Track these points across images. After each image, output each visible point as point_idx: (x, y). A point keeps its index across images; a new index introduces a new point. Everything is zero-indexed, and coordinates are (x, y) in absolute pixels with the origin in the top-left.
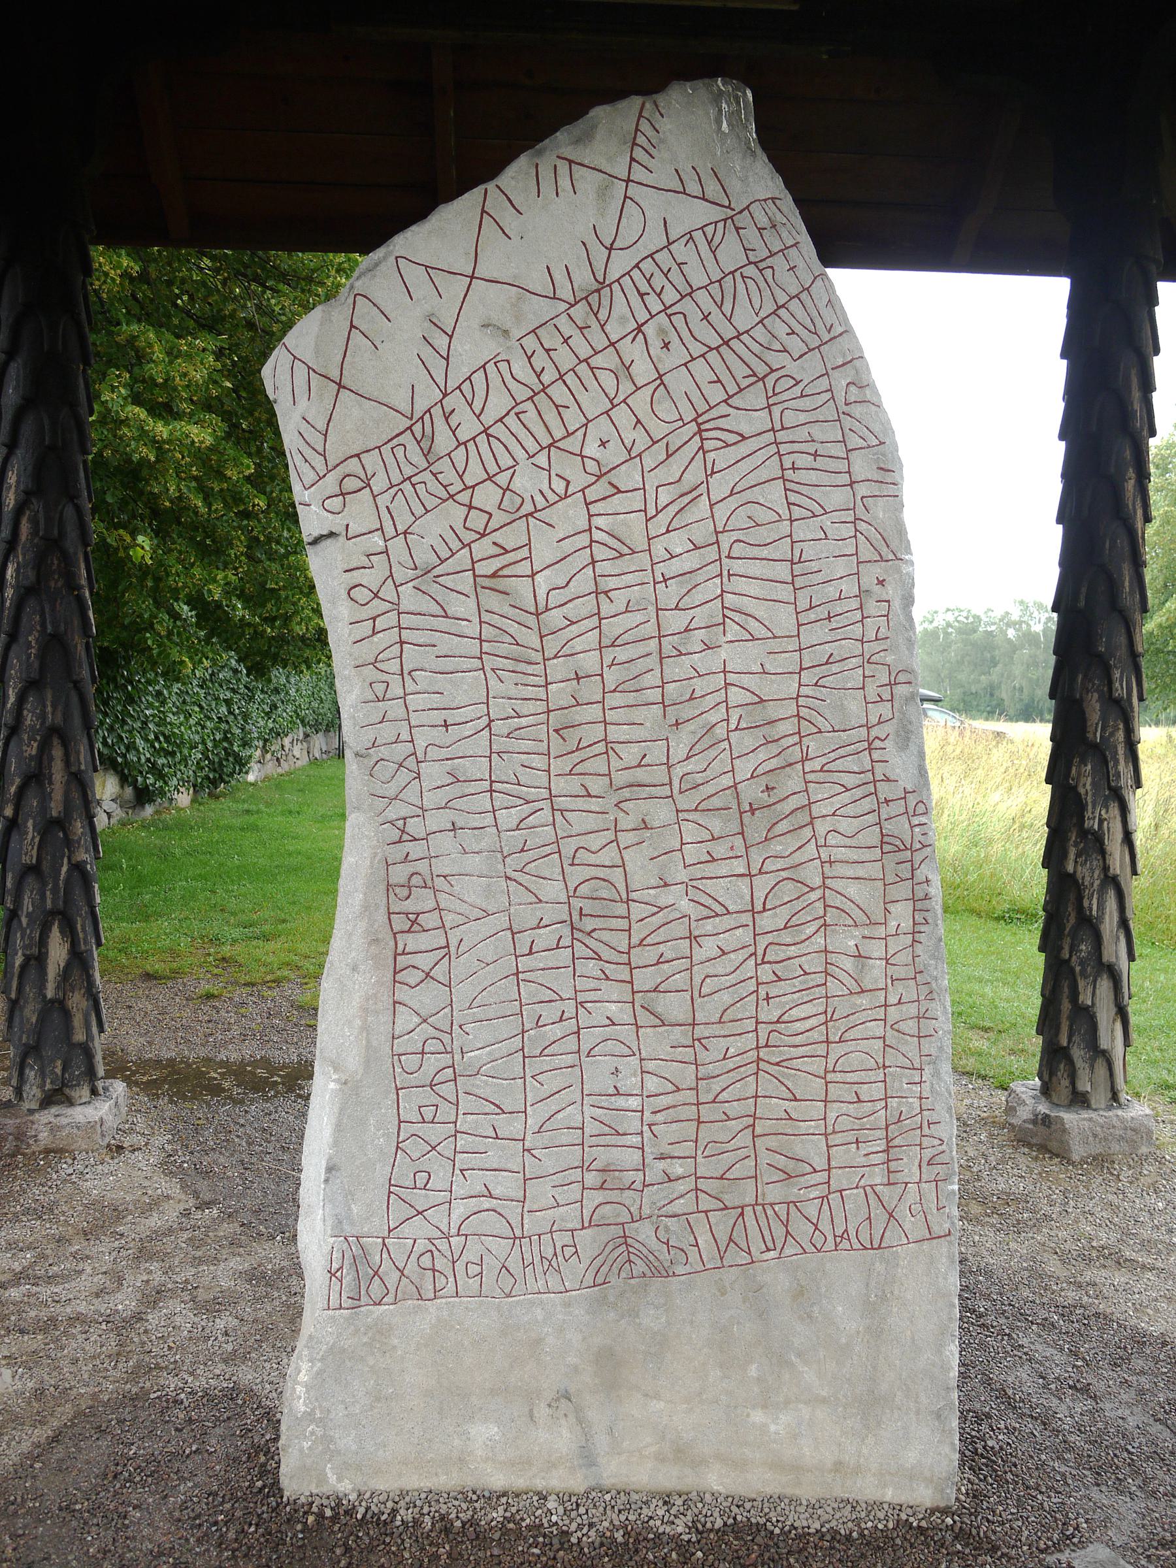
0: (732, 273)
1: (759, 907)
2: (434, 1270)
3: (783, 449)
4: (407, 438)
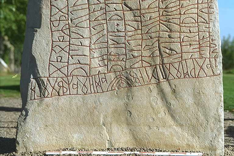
2: (63, 87)
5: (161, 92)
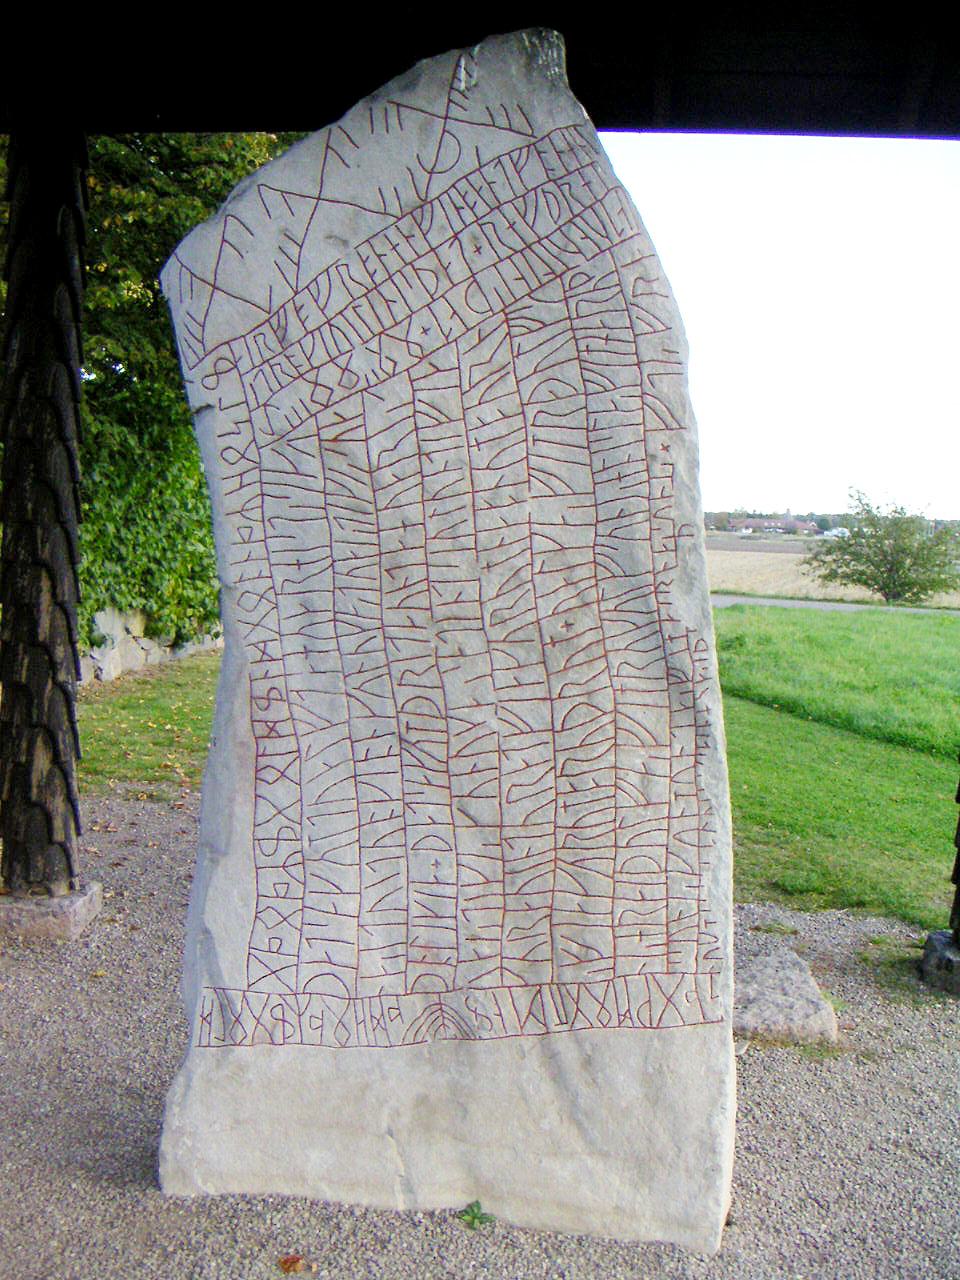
0: (535, 189)
1: (558, 727)
2: (284, 1021)
3: (580, 334)
4: (266, 329)
5: (551, 1057)
